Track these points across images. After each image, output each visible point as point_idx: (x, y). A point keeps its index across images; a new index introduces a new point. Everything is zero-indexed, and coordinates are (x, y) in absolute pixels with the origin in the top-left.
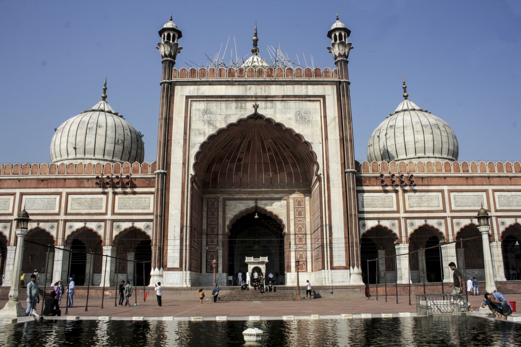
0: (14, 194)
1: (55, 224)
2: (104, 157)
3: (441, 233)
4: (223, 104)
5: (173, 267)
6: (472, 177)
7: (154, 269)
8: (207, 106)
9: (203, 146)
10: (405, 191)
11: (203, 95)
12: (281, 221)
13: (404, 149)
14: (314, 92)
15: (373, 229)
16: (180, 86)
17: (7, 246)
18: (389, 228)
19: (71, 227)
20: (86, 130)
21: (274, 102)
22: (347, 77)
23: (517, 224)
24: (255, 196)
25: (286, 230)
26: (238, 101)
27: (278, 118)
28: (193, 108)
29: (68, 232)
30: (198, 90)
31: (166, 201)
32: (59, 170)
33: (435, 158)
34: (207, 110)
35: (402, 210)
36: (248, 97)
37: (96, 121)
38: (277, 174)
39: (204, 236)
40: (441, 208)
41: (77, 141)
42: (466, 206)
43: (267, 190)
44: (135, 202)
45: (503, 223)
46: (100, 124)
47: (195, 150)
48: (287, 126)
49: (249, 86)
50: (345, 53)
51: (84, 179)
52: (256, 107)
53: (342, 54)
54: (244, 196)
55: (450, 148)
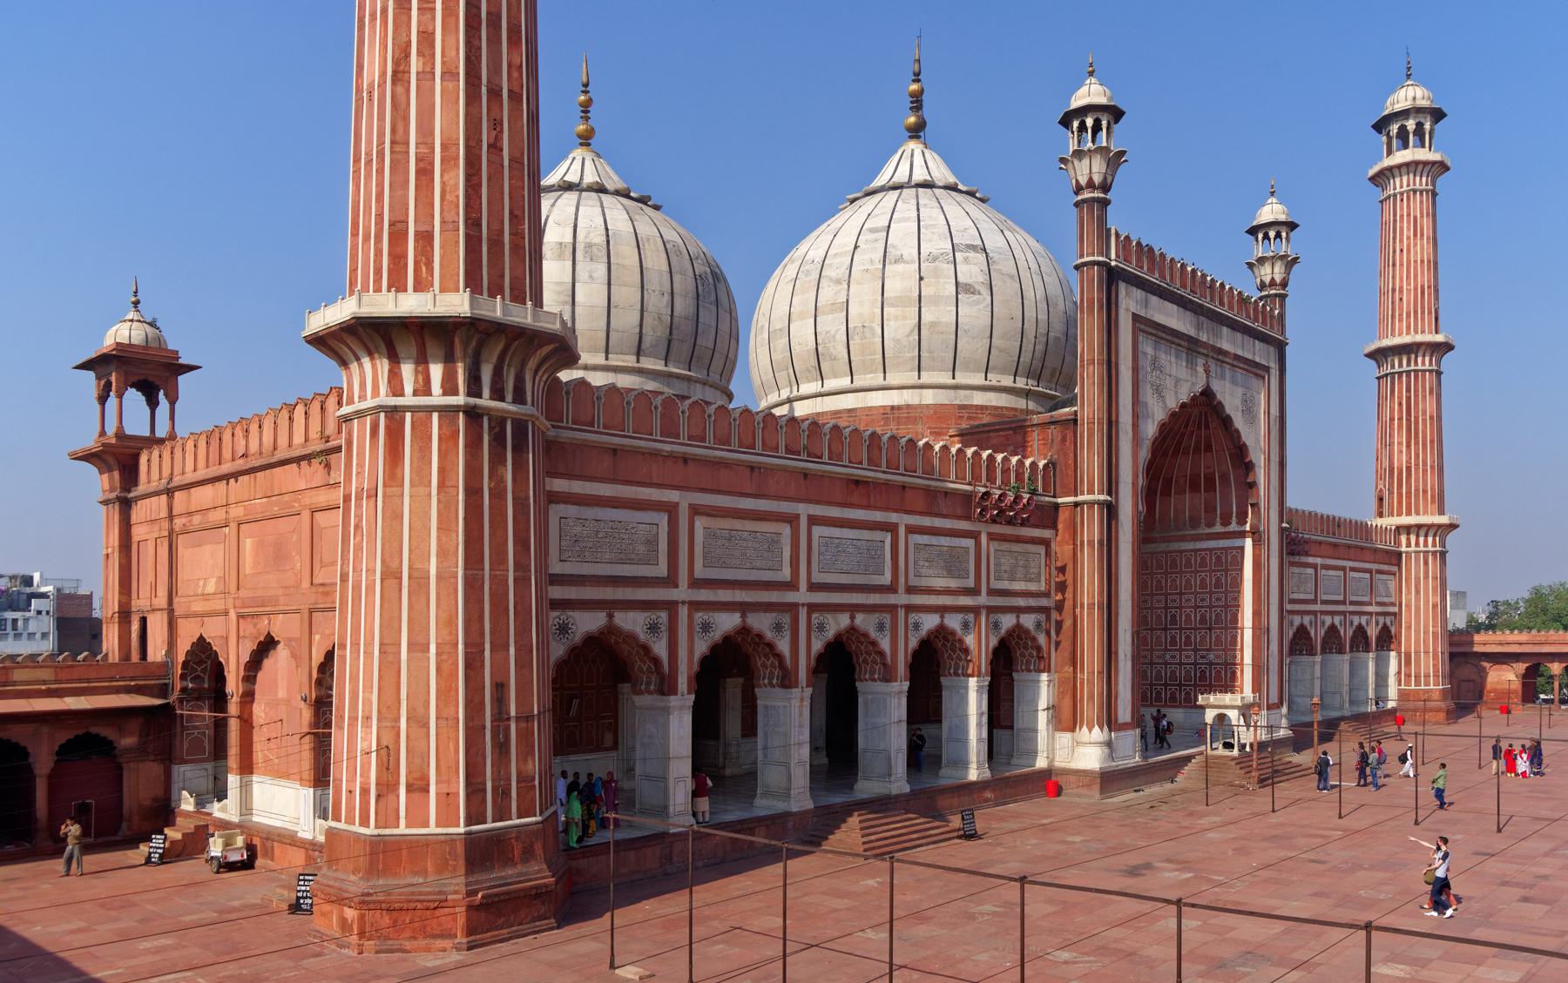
0: (792, 520)
21: (1224, 365)
32: (888, 455)
36: (1204, 345)
49: (1201, 317)
52: (1207, 371)
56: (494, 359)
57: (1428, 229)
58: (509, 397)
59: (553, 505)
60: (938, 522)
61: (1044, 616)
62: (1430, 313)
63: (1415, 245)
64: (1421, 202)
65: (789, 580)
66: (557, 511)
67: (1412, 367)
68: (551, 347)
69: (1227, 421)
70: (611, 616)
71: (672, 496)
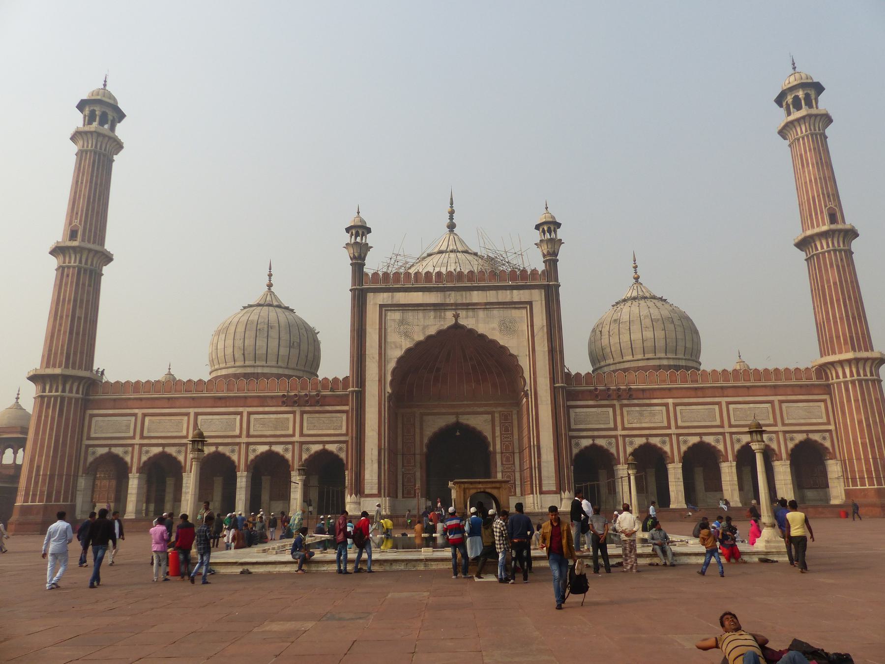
0: (188, 414)
1: (237, 448)
2: (277, 364)
3: (665, 453)
4: (421, 314)
5: (371, 493)
6: (702, 388)
7: (351, 496)
8: (402, 315)
9: (400, 360)
10: (622, 406)
11: (398, 303)
12: (485, 438)
13: (631, 349)
14: (520, 298)
15: (586, 448)
16: (372, 294)
17: (182, 473)
18: (606, 447)
19: (254, 450)
21: (476, 310)
22: (556, 279)
24: (456, 410)
25: (491, 449)
26: (437, 310)
27: (481, 329)
28: (388, 318)
29: (251, 456)
30: (392, 297)
31: (362, 421)
33: (668, 358)
34: (403, 320)
36: (447, 305)
38: (480, 385)
39: (400, 457)
40: (665, 424)
41: (245, 345)
43: (469, 402)
45: (739, 441)
46: (271, 324)
47: (391, 365)
48: (490, 337)
49: (448, 293)
50: (554, 251)
52: (456, 316)
53: (551, 253)
54: (444, 411)
55: (687, 346)
56: (49, 383)
57: (811, 158)
58: (54, 391)
59: (94, 418)
60: (267, 409)
62: (822, 212)
63: (804, 172)
64: (804, 144)
65: (185, 435)
66: (94, 419)
67: (815, 252)
68: (60, 378)
69: (483, 337)
70: (110, 449)
71: (136, 411)
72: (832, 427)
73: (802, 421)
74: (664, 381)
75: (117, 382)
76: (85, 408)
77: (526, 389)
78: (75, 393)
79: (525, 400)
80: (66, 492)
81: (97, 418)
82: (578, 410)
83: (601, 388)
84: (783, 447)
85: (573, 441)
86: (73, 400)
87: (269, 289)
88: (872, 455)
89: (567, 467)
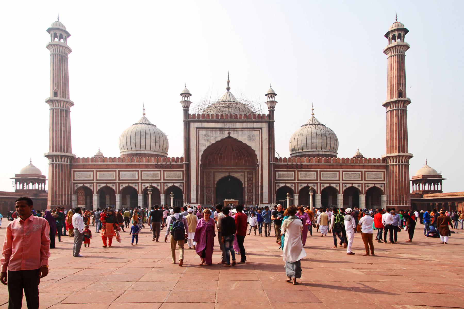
0: (115, 171)
1: (137, 184)
10: (298, 171)
15: (282, 187)
18: (290, 187)
20: (140, 136)
23: (352, 187)
32: (136, 160)
35: (296, 179)
37: (145, 131)
40: (316, 179)
42: (328, 178)
44: (174, 175)
45: (345, 186)
48: (244, 142)
51: (149, 164)
52: (229, 133)
60: (149, 169)
61: (182, 184)
69: (241, 142)
71: (93, 170)
72: (385, 182)
73: (373, 179)
74: (317, 162)
75: (83, 158)
76: (71, 169)
77: (258, 164)
78: (66, 162)
79: (257, 168)
80: (68, 201)
81: (76, 172)
82: (280, 172)
83: (290, 164)
84: (364, 189)
85: (277, 184)
86: (66, 165)
87: (144, 116)
88: (399, 194)
89: (273, 194)
